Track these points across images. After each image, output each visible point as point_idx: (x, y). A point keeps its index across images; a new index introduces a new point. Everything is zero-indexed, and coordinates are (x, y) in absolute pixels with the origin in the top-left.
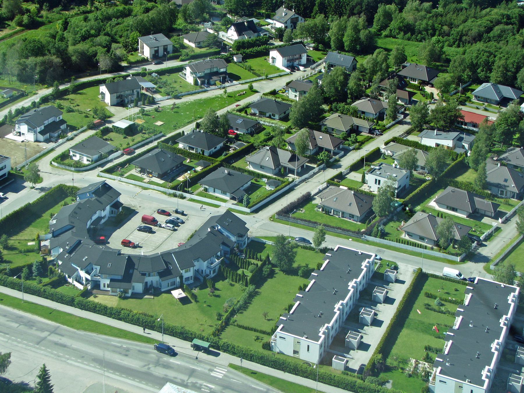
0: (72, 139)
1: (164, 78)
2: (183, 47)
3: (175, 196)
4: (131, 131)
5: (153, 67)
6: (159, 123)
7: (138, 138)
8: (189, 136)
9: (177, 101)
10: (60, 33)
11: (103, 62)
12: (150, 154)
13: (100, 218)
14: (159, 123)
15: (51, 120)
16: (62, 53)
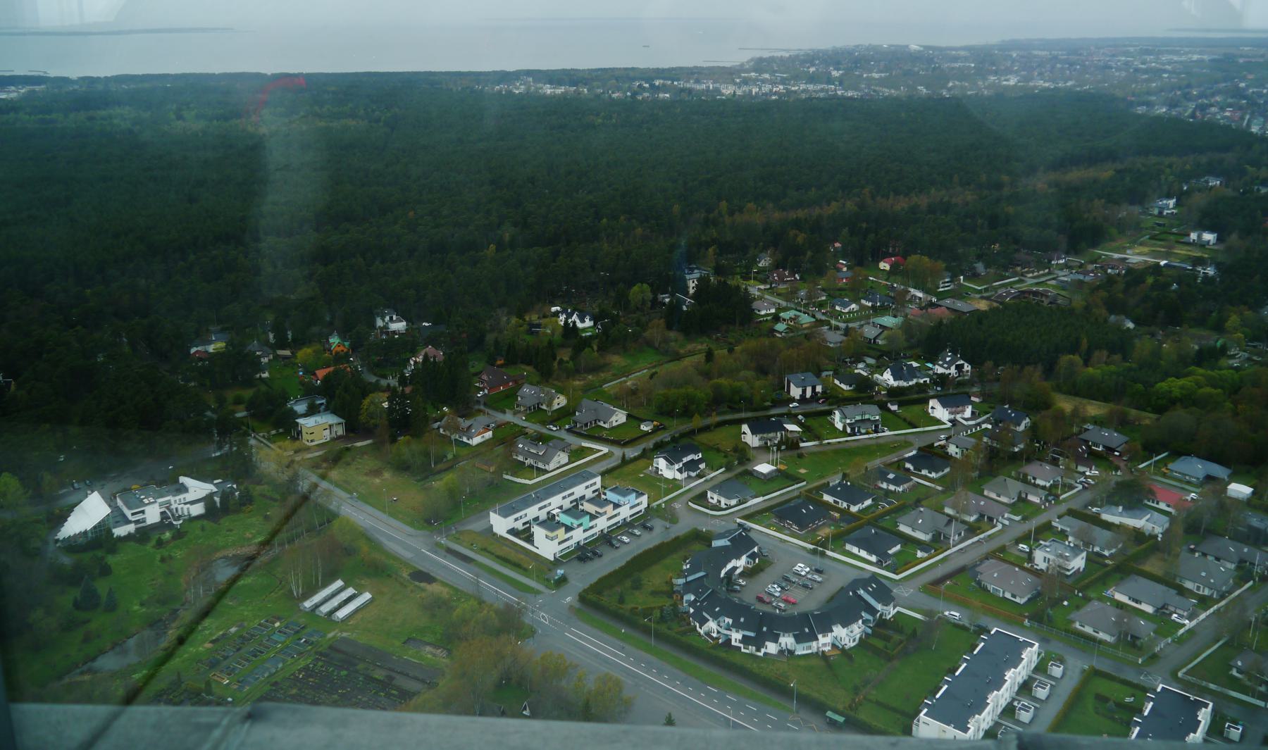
3: (814, 552)
13: (735, 568)
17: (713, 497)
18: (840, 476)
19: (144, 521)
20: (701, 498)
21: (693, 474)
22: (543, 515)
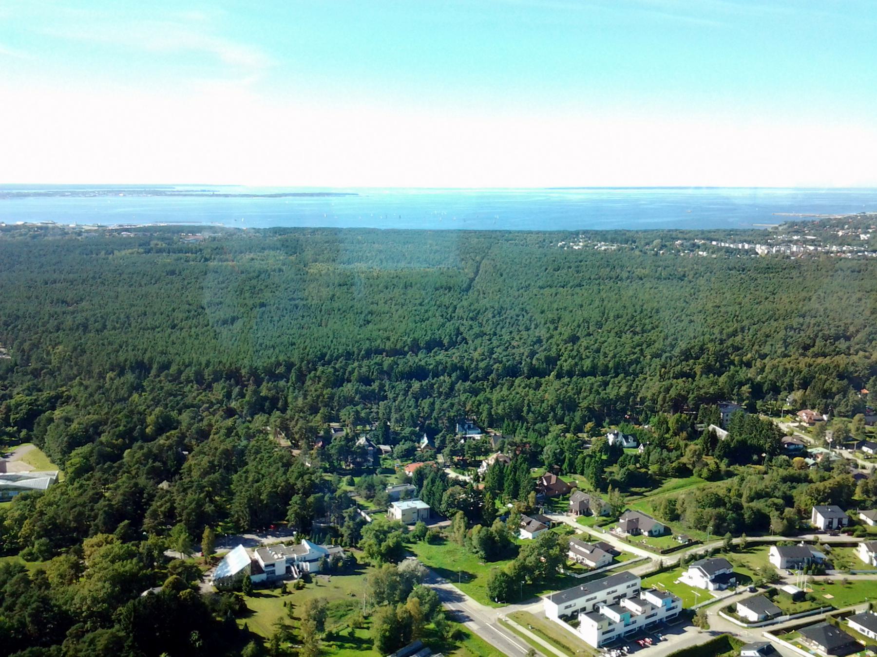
0: (740, 593)
1: (838, 550)
2: (861, 522)
4: (800, 597)
5: (826, 538)
6: (829, 596)
7: (806, 605)
8: (861, 616)
9: (851, 578)
10: (736, 487)
11: (776, 524)
12: (817, 626)
14: (829, 596)
15: (721, 572)
16: (738, 507)
17: (743, 611)
18: (866, 606)
19: (273, 572)
20: (731, 610)
21: (724, 586)
22: (589, 606)
